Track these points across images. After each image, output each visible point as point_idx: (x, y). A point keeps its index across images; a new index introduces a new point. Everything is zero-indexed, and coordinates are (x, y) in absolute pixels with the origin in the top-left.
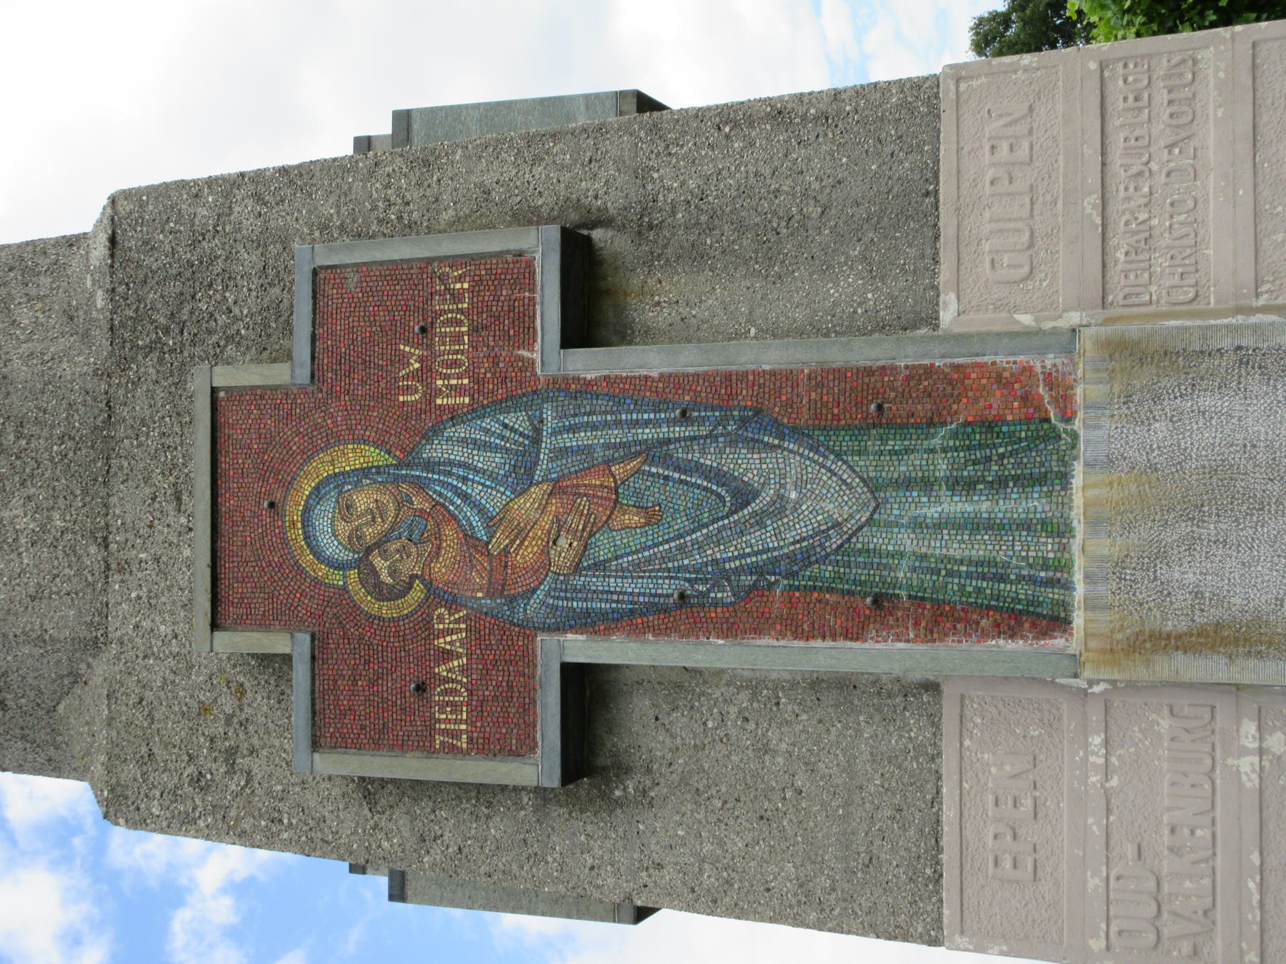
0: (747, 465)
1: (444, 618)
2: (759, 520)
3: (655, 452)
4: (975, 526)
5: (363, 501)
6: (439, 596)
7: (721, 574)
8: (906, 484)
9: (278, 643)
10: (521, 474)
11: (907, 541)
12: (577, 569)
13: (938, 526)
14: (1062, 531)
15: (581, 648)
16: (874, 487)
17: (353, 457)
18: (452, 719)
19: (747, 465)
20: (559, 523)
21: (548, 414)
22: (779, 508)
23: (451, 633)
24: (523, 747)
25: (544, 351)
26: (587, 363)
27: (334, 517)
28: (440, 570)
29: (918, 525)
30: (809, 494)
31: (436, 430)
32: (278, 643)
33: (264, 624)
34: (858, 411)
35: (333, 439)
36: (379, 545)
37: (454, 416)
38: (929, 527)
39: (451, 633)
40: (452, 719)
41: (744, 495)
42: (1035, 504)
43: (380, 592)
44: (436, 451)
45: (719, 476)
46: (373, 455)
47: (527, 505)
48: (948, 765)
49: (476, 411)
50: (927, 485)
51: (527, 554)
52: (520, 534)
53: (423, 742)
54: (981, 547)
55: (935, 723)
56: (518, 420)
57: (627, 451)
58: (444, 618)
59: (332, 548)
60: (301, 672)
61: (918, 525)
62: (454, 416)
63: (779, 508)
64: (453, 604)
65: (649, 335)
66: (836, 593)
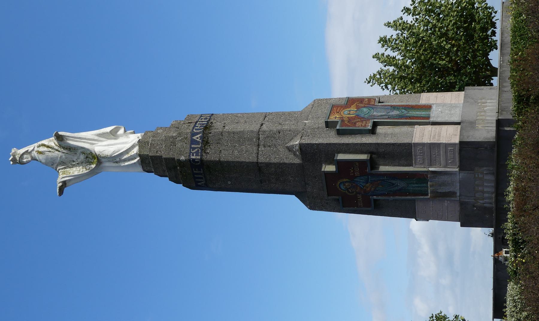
0: (394, 182)
2: (395, 187)
4: (418, 187)
5: (346, 184)
9: (337, 197)
10: (367, 182)
17: (345, 180)
19: (394, 182)
22: (397, 185)
23: (359, 196)
27: (343, 185)
30: (401, 184)
32: (337, 197)
36: (349, 188)
37: (358, 176)
39: (359, 196)
41: (393, 184)
42: (425, 185)
43: (350, 192)
44: (356, 180)
46: (347, 180)
47: (368, 185)
50: (413, 184)
51: (368, 189)
54: (419, 189)
56: (366, 177)
60: (341, 201)
62: (358, 176)
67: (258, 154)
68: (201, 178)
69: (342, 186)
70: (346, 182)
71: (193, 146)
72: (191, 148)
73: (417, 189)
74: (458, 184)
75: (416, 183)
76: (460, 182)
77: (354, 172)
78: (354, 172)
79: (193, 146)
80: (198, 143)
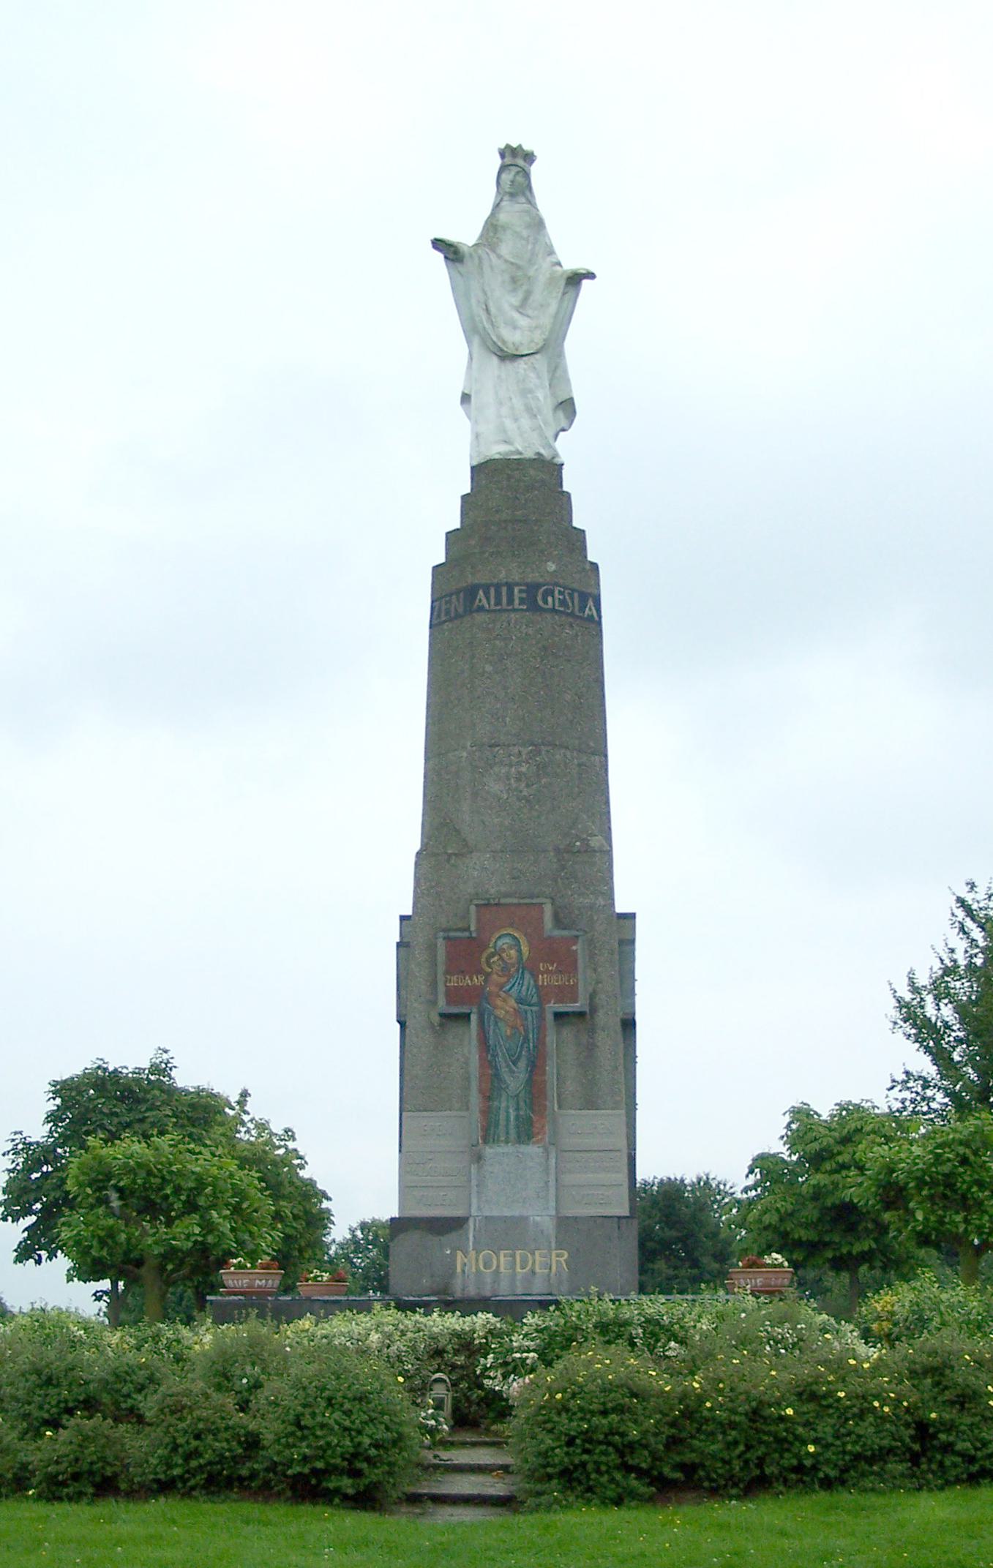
0: (522, 1064)
1: (481, 978)
2: (508, 1066)
3: (526, 1039)
4: (508, 1120)
5: (513, 952)
6: (488, 975)
7: (495, 1056)
8: (518, 1104)
10: (520, 1001)
11: (503, 1105)
12: (496, 1017)
13: (508, 1112)
14: (507, 1142)
15: (474, 1018)
16: (517, 1096)
17: (525, 949)
18: (454, 981)
20: (507, 1012)
21: (534, 1009)
23: (478, 980)
24: (449, 1003)
25: (553, 1006)
26: (549, 1018)
27: (509, 944)
28: (495, 976)
29: (508, 1107)
30: (515, 1080)
31: (532, 975)
33: (479, 920)
34: (535, 1092)
35: (530, 944)
36: (501, 958)
38: (507, 1110)
39: (478, 980)
40: (454, 981)
41: (515, 1063)
44: (527, 976)
45: (519, 1058)
46: (525, 958)
47: (512, 1002)
48: (448, 1113)
49: (536, 986)
50: (517, 1109)
51: (499, 1002)
52: (504, 1001)
53: (448, 972)
54: (502, 1122)
55: (460, 1109)
56: (535, 999)
57: (526, 1031)
58: (481, 978)
59: (500, 943)
61: (508, 1107)
62: (536, 981)
63: (512, 1072)
64: (485, 981)
65: (558, 1033)
66: (492, 1087)
67: (567, 748)
68: (498, 602)
69: (507, 940)
70: (519, 951)
71: (576, 595)
72: (573, 590)
73: (502, 1117)
74: (517, 1214)
75: (517, 1117)
76: (524, 1219)
77: (548, 972)
78: (548, 972)
79: (576, 595)
80: (582, 609)
